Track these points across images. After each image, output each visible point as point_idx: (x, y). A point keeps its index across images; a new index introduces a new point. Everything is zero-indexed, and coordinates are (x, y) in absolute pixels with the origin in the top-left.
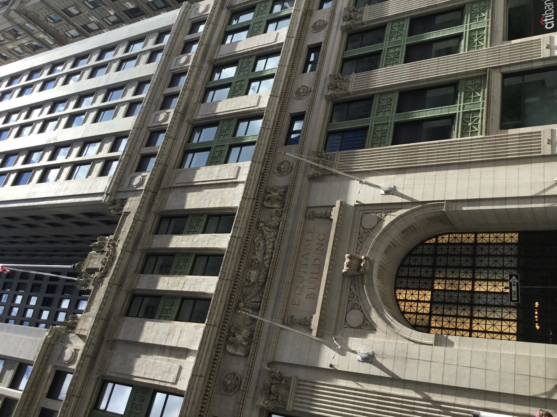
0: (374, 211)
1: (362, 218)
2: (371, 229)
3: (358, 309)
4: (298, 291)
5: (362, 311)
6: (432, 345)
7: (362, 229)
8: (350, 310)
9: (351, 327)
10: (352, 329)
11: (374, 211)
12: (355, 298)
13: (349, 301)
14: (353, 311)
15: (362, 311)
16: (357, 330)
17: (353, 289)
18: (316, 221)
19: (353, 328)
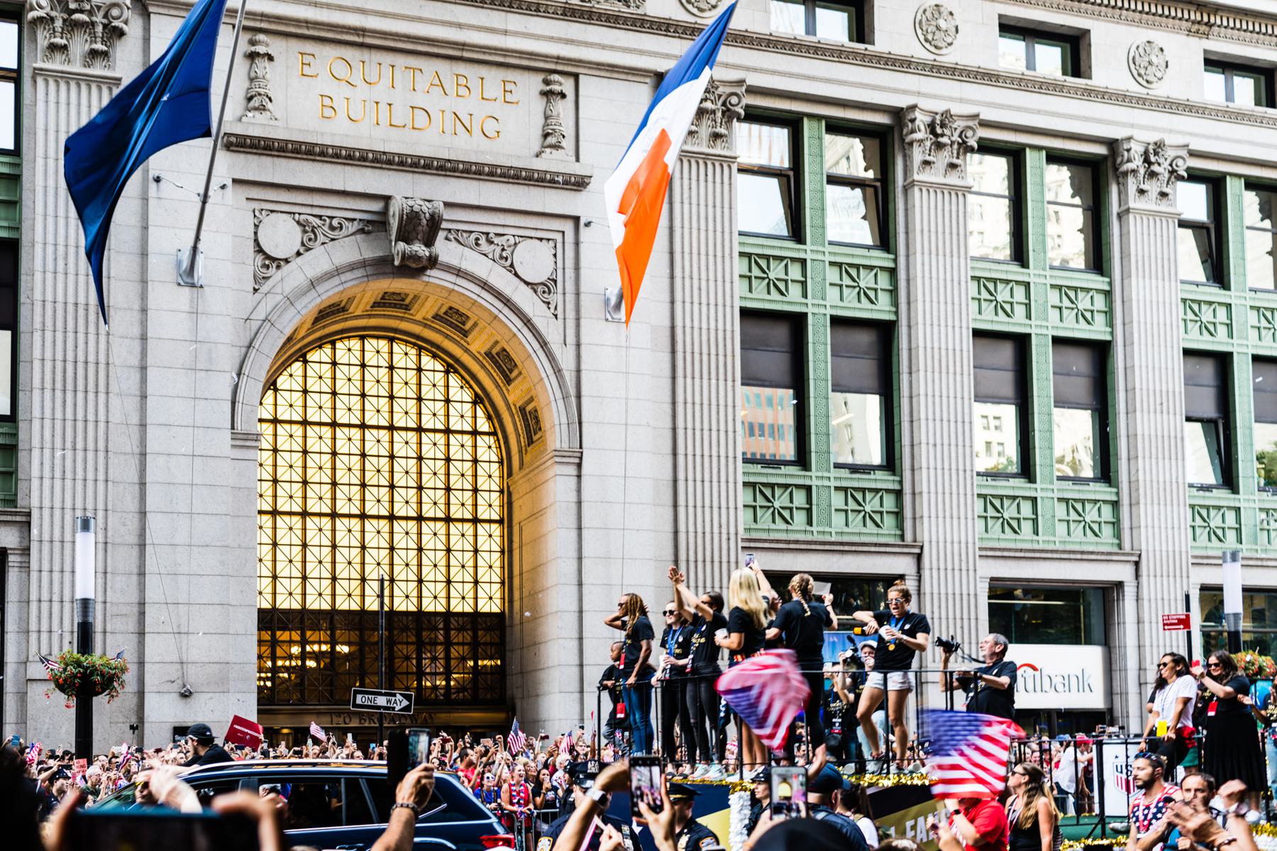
0: (560, 272)
1: (541, 239)
2: (512, 265)
3: (303, 244)
4: (341, 70)
5: (299, 254)
6: (233, 428)
7: (512, 241)
8: (298, 223)
9: (256, 226)
10: (252, 229)
11: (560, 272)
12: (332, 234)
13: (320, 217)
14: (298, 229)
15: (299, 254)
16: (252, 243)
17: (353, 227)
18: (539, 104)
19: (256, 233)
